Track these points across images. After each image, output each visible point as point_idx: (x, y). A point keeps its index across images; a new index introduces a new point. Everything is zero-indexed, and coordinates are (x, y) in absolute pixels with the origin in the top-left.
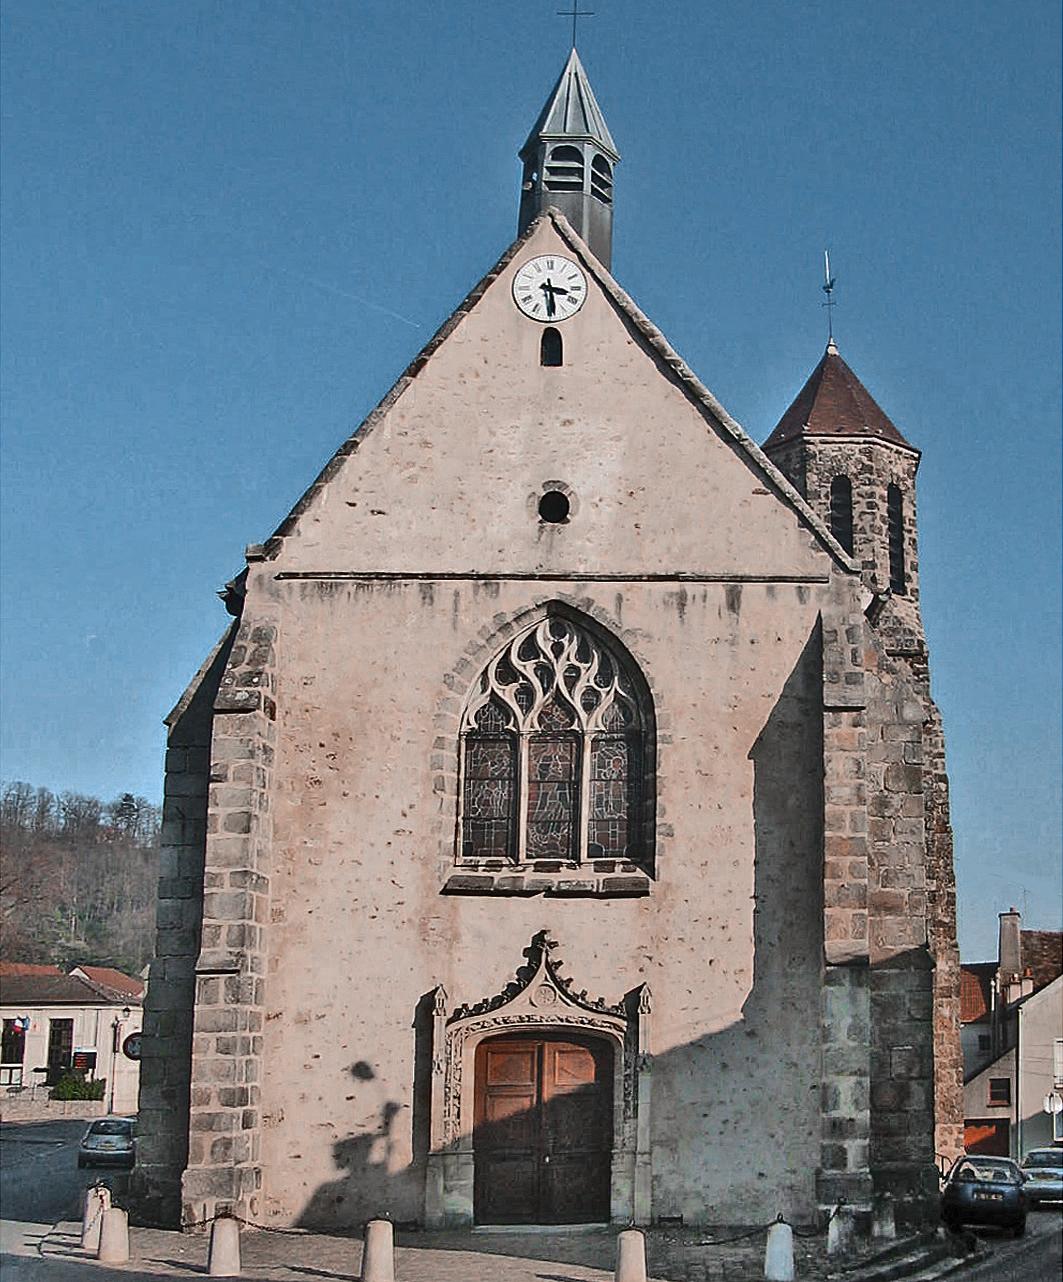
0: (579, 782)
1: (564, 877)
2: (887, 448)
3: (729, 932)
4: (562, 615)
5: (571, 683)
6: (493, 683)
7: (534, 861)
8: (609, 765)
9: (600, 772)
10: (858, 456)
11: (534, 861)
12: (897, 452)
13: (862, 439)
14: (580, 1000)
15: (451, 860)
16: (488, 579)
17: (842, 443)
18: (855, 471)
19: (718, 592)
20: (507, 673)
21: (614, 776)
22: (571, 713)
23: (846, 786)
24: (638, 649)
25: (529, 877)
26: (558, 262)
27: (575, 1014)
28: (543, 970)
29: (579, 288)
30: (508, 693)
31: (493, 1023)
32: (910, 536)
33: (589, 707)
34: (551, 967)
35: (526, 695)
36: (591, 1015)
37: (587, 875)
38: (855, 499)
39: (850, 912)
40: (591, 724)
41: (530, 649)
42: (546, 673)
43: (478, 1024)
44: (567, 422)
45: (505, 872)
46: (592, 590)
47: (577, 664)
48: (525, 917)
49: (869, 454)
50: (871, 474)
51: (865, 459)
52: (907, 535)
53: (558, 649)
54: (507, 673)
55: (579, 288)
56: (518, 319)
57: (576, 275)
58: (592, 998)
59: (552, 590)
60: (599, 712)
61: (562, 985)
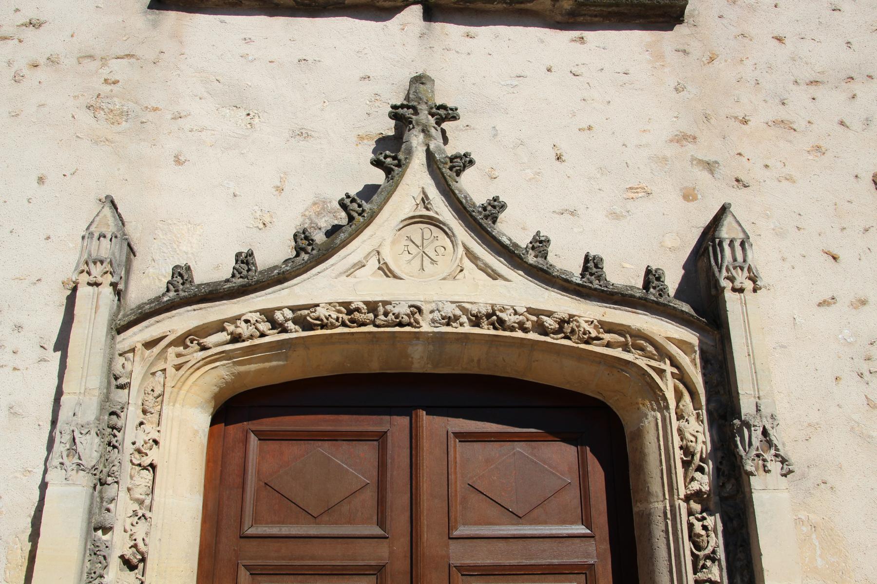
14: (531, 259)
27: (518, 294)
28: (417, 178)
31: (264, 327)
34: (446, 171)
36: (561, 304)
43: (219, 327)
58: (566, 260)
61: (481, 221)
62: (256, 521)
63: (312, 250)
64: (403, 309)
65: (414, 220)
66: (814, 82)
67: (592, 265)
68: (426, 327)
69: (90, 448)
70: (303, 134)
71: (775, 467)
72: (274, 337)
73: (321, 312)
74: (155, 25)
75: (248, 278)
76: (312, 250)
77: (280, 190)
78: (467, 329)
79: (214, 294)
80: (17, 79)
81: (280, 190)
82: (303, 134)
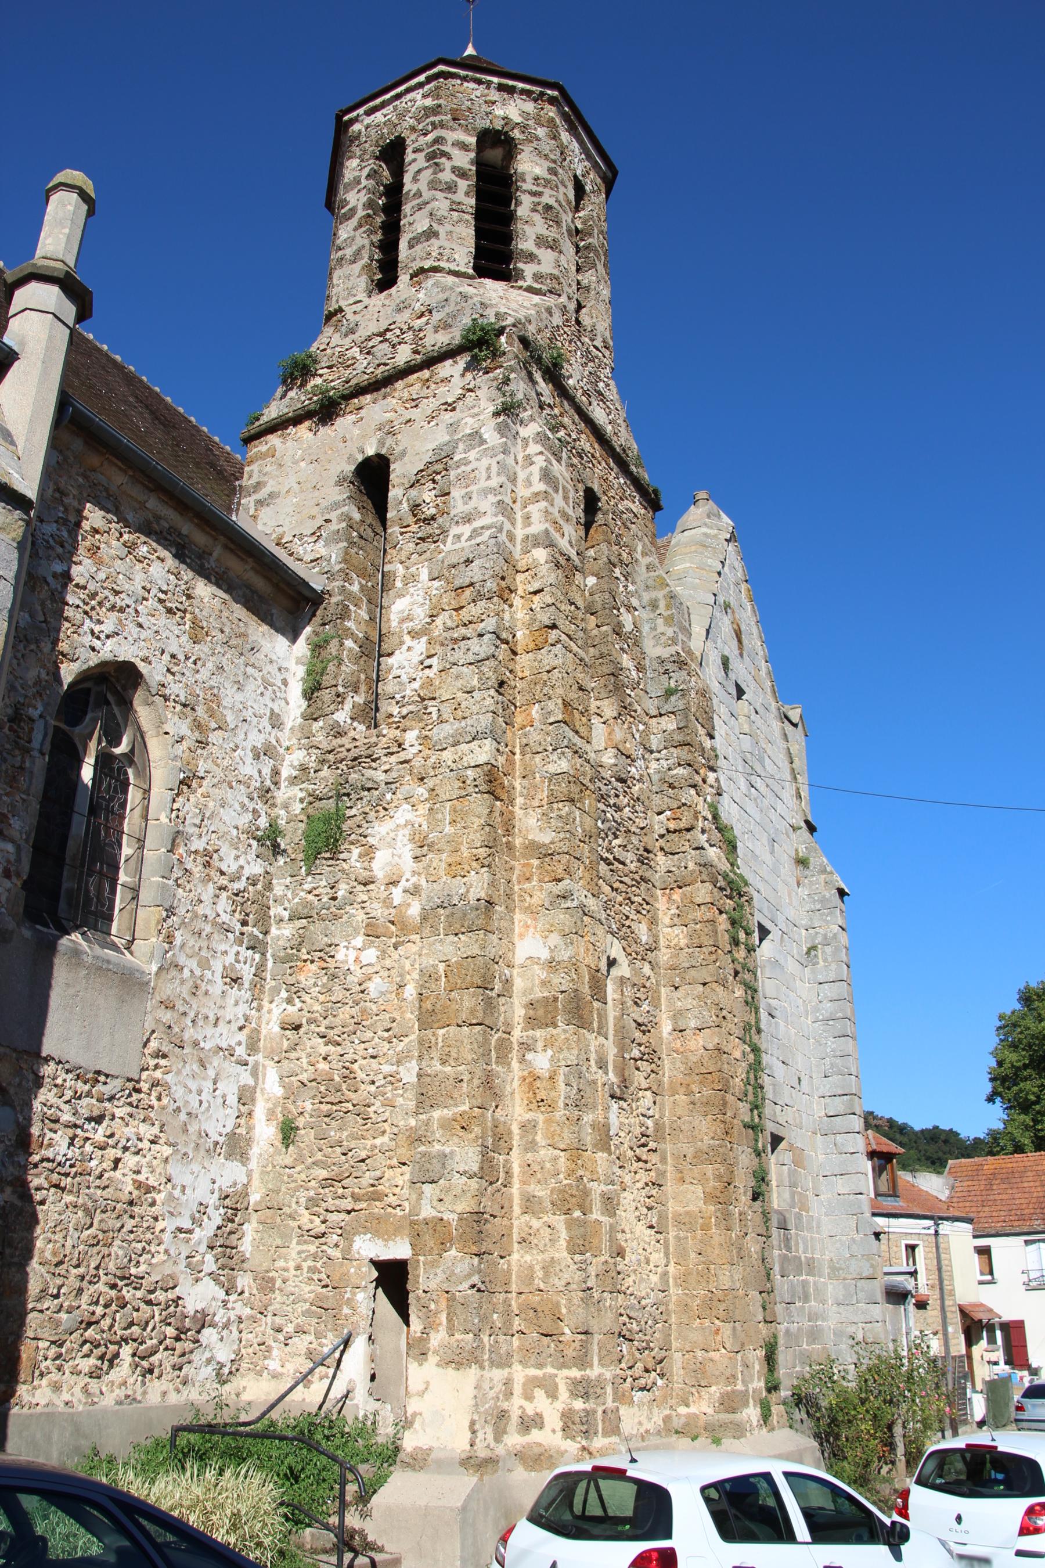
2: (479, 82)
12: (501, 88)
13: (422, 78)
17: (398, 97)
32: (536, 200)
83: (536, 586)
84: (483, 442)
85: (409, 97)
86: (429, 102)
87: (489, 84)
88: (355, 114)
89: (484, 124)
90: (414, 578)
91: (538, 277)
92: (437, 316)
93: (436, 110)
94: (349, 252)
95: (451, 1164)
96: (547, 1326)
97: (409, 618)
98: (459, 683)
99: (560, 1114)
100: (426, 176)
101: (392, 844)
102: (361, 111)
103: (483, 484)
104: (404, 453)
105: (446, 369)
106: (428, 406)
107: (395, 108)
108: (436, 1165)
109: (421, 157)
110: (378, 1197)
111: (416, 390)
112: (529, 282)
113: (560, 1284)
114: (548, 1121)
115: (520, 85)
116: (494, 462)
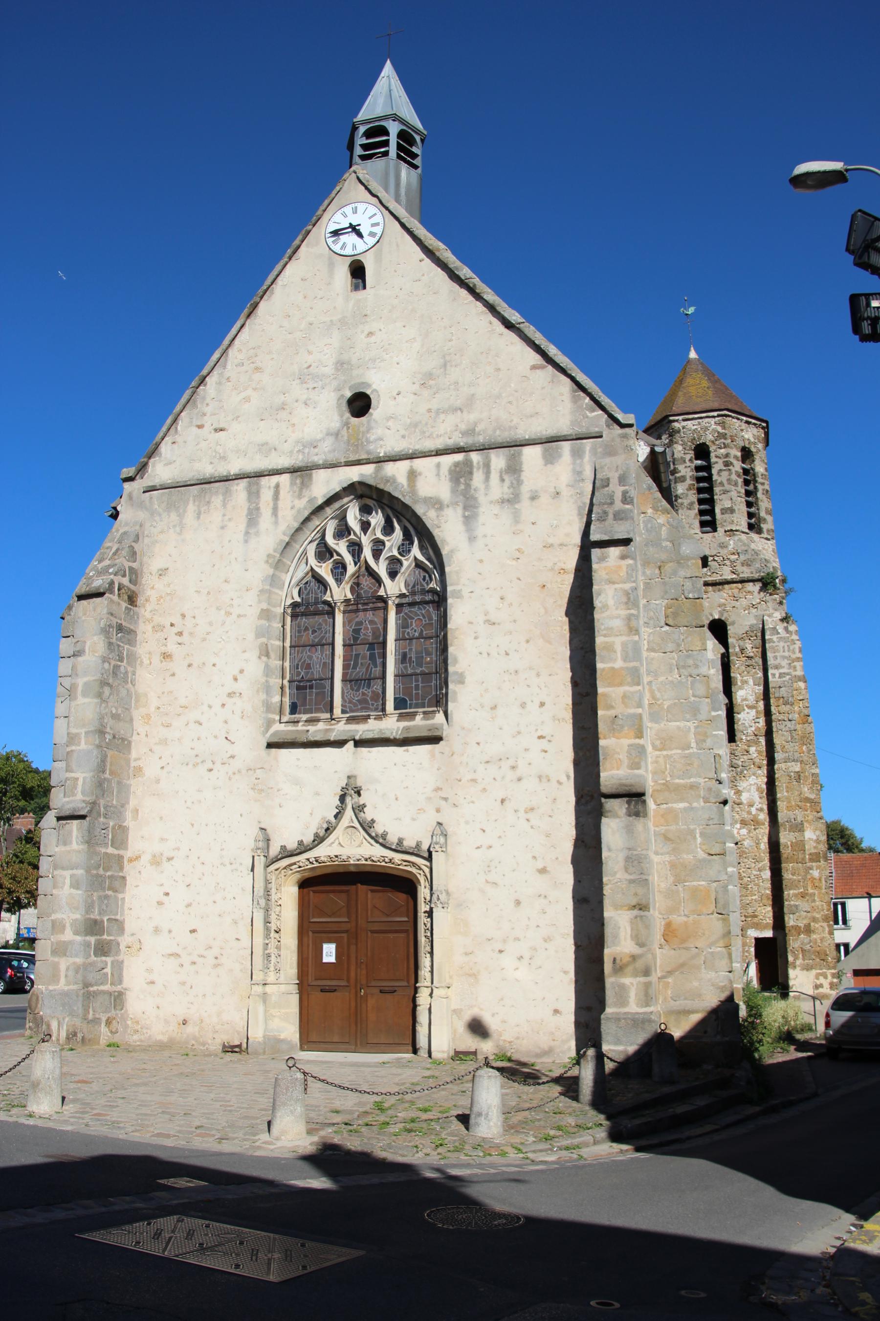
0: (384, 643)
1: (372, 728)
2: (738, 419)
3: (519, 773)
4: (370, 496)
5: (377, 554)
6: (313, 561)
7: (348, 715)
8: (412, 625)
9: (404, 633)
10: (713, 427)
11: (348, 715)
12: (747, 422)
13: (715, 414)
14: (381, 840)
15: (277, 718)
16: (301, 472)
18: (713, 439)
19: (498, 460)
20: (324, 552)
21: (417, 634)
22: (379, 581)
23: (617, 618)
24: (429, 517)
25: (341, 729)
26: (361, 207)
27: (377, 852)
28: (349, 813)
29: (377, 224)
30: (325, 570)
31: (307, 863)
33: (393, 574)
35: (340, 568)
37: (391, 724)
38: (713, 459)
39: (626, 742)
40: (393, 588)
41: (343, 531)
42: (356, 548)
43: (295, 864)
44: (370, 334)
45: (321, 726)
46: (390, 469)
47: (382, 537)
48: (335, 764)
49: (723, 425)
50: (725, 439)
51: (719, 429)
52: (760, 487)
53: (365, 526)
54: (324, 552)
55: (377, 224)
56: (330, 258)
57: (375, 214)
58: (393, 839)
59: (354, 474)
60: (400, 579)
61: (367, 827)
62: (313, 917)
63: (319, 840)
64: (345, 857)
65: (348, 827)
66: (488, 762)
67: (400, 841)
68: (352, 862)
69: (263, 902)
70: (317, 794)
71: (440, 906)
72: (310, 866)
73: (322, 859)
74: (269, 754)
75: (303, 848)
76: (319, 840)
77: (311, 814)
78: (364, 862)
79: (292, 855)
80: (230, 779)
81: (311, 814)
82: (317, 794)
83: (801, 698)
84: (778, 633)
85: (707, 420)
86: (719, 429)
87: (742, 420)
88: (676, 418)
89: (742, 444)
90: (746, 682)
91: (768, 531)
92: (743, 557)
93: (723, 436)
94: (686, 502)
95: (800, 908)
96: (823, 957)
97: (746, 700)
98: (783, 738)
99: (824, 891)
100: (725, 474)
101: (749, 791)
102: (680, 418)
103: (781, 653)
104: (733, 623)
105: (750, 586)
106: (744, 602)
107: (699, 424)
108: (794, 908)
109: (720, 461)
110: (756, 916)
111: (736, 591)
112: (765, 535)
113: (826, 944)
114: (819, 893)
115: (753, 421)
116: (786, 645)
